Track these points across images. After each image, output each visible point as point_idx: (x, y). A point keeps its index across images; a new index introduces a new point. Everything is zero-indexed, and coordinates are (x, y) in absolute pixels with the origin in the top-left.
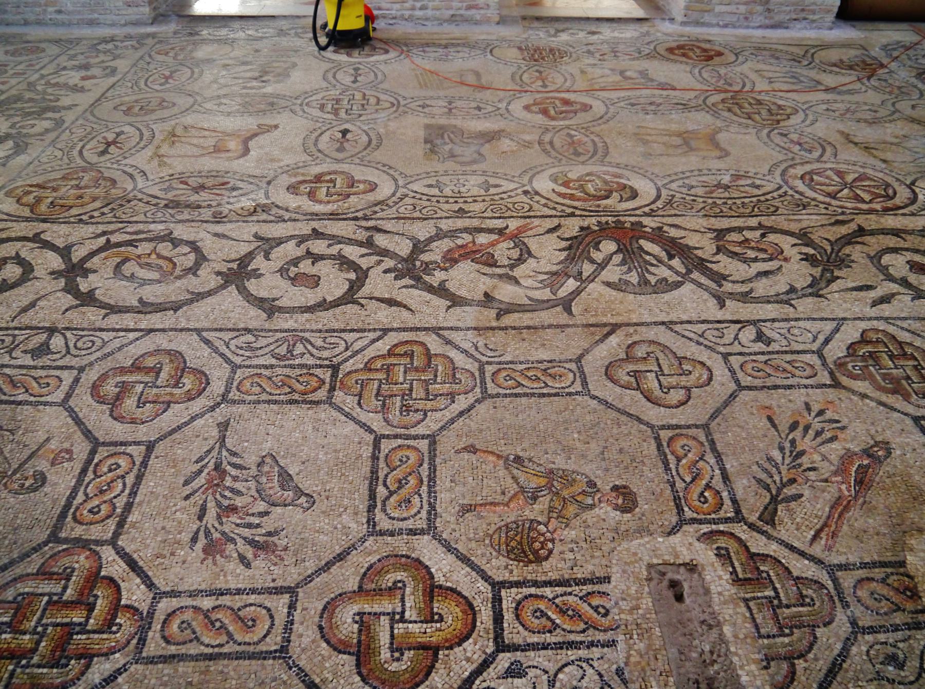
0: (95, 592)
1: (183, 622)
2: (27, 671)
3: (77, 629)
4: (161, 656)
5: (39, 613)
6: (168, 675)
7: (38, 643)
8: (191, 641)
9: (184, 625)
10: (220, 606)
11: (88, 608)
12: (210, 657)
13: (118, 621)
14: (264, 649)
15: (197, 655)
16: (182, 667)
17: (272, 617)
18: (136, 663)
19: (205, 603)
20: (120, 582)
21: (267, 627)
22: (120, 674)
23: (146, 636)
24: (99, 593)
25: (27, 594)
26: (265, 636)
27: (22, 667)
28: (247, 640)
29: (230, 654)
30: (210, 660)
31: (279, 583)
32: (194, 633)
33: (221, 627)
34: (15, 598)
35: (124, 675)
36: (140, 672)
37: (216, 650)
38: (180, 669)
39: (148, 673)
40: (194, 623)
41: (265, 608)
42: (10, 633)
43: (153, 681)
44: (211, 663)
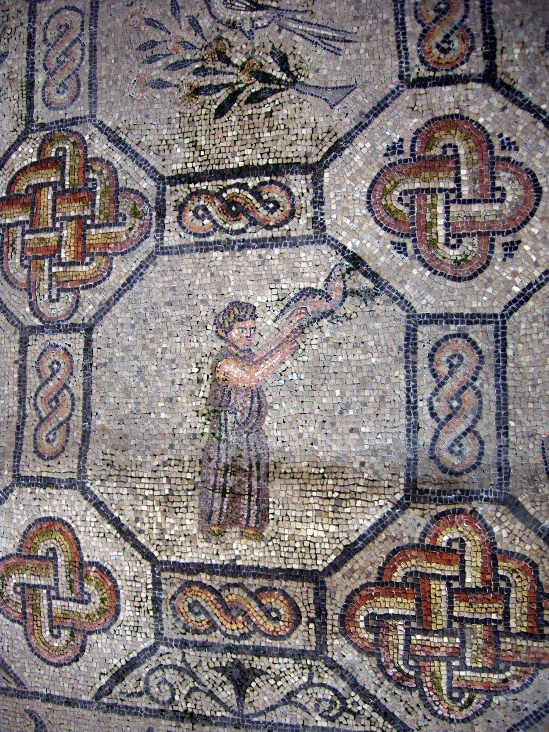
0: (23, 192)
1: (58, 92)
2: (97, 214)
3: (59, 188)
4: (90, 97)
5: (43, 235)
6: (107, 83)
7: (72, 218)
8: (77, 76)
9: (61, 89)
10: (44, 64)
11: (38, 191)
12: (93, 49)
13: (53, 155)
14: (88, 6)
15: (91, 65)
16: (102, 72)
17: (58, 11)
18: (95, 116)
19: (40, 80)
20: (14, 173)
21: (67, 12)
22: (104, 126)
23: (69, 119)
24: (24, 187)
25: (21, 257)
26: (77, 10)
27: (93, 221)
28: (79, 25)
29: (91, 35)
30: (96, 50)
31: (25, 17)
32: (69, 76)
33: (65, 54)
34: (26, 267)
35: (105, 122)
36: (103, 109)
37: (87, 50)
38: (103, 73)
39: (104, 101)
40: (60, 81)
41: (49, 21)
42: (60, 252)
43: (113, 93)
44: (98, 48)
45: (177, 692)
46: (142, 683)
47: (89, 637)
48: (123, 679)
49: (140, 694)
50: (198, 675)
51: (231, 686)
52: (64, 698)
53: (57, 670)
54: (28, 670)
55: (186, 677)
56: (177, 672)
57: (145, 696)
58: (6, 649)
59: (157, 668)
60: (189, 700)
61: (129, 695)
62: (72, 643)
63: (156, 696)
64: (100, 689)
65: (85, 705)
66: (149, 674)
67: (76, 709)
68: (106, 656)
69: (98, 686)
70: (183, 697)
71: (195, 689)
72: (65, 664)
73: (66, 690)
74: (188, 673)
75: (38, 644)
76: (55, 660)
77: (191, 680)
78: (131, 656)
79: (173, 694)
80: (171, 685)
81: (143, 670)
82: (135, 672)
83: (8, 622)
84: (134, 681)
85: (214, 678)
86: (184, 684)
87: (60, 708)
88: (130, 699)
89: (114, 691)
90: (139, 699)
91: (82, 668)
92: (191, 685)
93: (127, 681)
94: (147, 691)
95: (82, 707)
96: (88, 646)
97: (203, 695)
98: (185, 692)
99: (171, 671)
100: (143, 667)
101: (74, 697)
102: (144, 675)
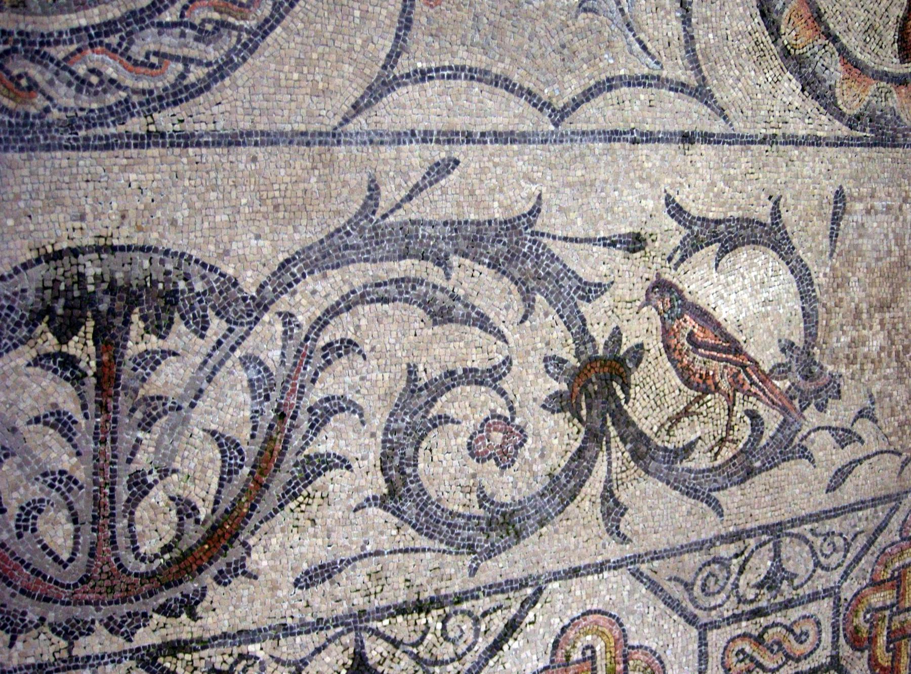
45: (439, 633)
46: (483, 628)
47: (548, 663)
48: (506, 626)
49: (485, 614)
50: (413, 663)
51: (370, 663)
52: (582, 575)
53: (588, 607)
54: (625, 593)
55: (427, 656)
56: (440, 658)
57: (479, 614)
58: (652, 608)
59: (464, 654)
60: (424, 628)
61: (500, 607)
62: (568, 648)
63: (466, 617)
64: (535, 603)
65: (556, 576)
66: (474, 644)
67: (566, 567)
68: (527, 646)
69: (538, 606)
70: (432, 630)
71: (416, 645)
72: (578, 618)
73: (578, 587)
74: (425, 662)
75: (611, 630)
76: (591, 618)
77: (422, 655)
78: (496, 658)
79: (444, 628)
80: (447, 639)
81: (482, 644)
82: (491, 640)
83: (646, 644)
84: (493, 629)
85: (393, 665)
86: (430, 646)
87: (587, 561)
88: (498, 604)
89: (518, 606)
90: (487, 607)
91: (558, 620)
92: (421, 648)
93: (502, 625)
94: (477, 621)
95: (559, 573)
96: (549, 651)
97: (406, 641)
98: (429, 636)
99: (446, 657)
100: (481, 650)
101: (569, 581)
102: (480, 640)
